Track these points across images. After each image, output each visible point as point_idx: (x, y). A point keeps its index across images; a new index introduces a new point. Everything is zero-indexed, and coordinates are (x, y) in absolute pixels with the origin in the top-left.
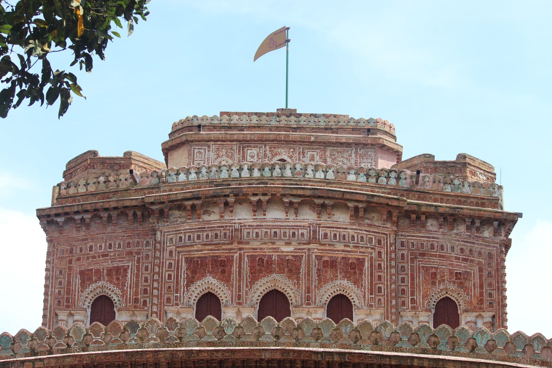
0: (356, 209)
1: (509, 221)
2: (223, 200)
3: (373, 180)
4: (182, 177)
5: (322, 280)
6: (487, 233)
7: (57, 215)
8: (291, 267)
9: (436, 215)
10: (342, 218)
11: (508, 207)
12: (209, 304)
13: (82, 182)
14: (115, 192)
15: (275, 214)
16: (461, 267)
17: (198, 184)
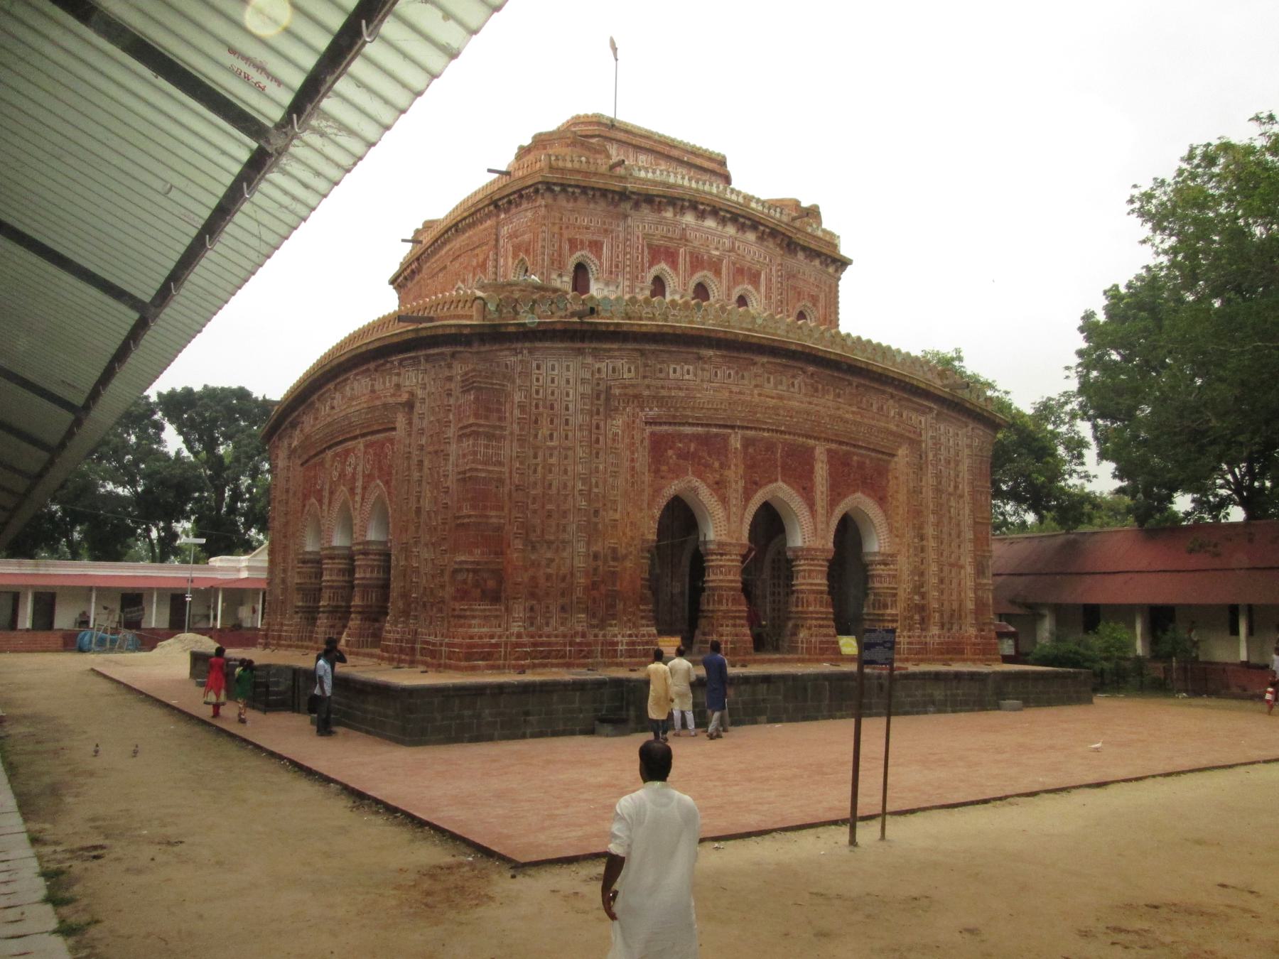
0: (763, 232)
1: (843, 263)
2: (679, 203)
3: (766, 211)
4: (642, 174)
5: (736, 283)
6: (831, 270)
7: (555, 184)
8: (716, 268)
9: (804, 249)
10: (751, 236)
11: (845, 250)
12: (659, 285)
13: (568, 158)
14: (595, 174)
15: (710, 223)
16: (814, 291)
17: (655, 183)
